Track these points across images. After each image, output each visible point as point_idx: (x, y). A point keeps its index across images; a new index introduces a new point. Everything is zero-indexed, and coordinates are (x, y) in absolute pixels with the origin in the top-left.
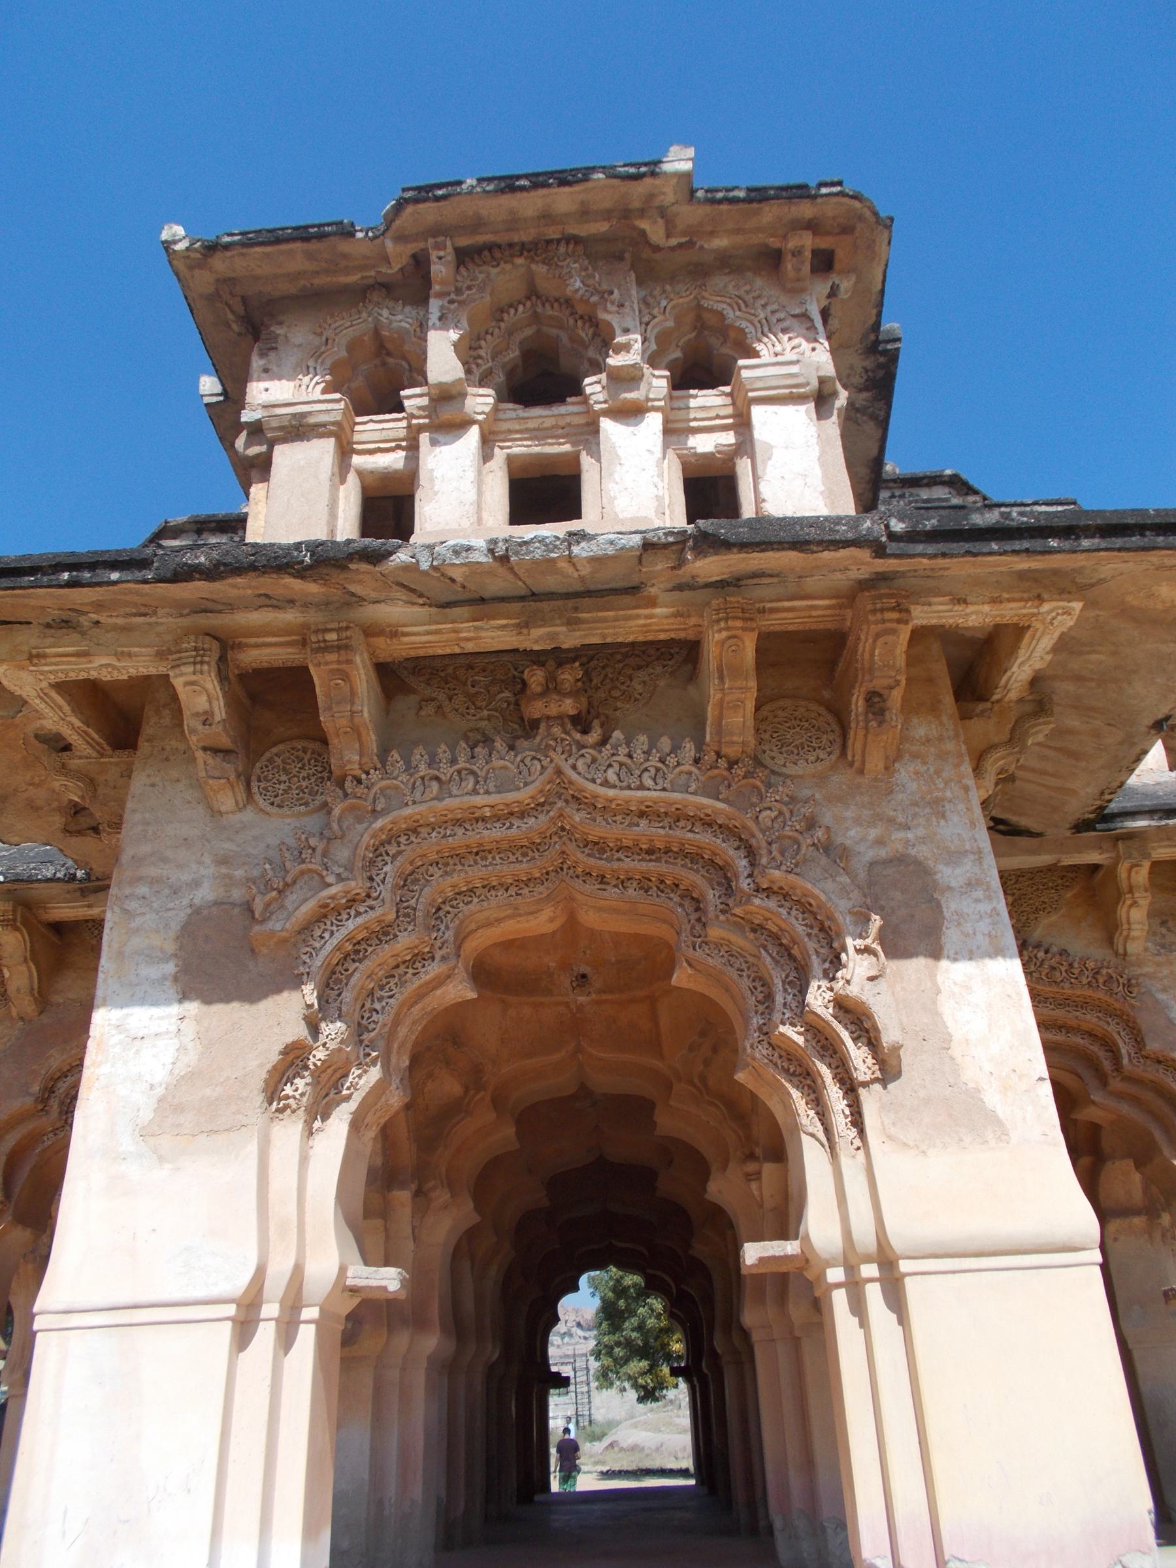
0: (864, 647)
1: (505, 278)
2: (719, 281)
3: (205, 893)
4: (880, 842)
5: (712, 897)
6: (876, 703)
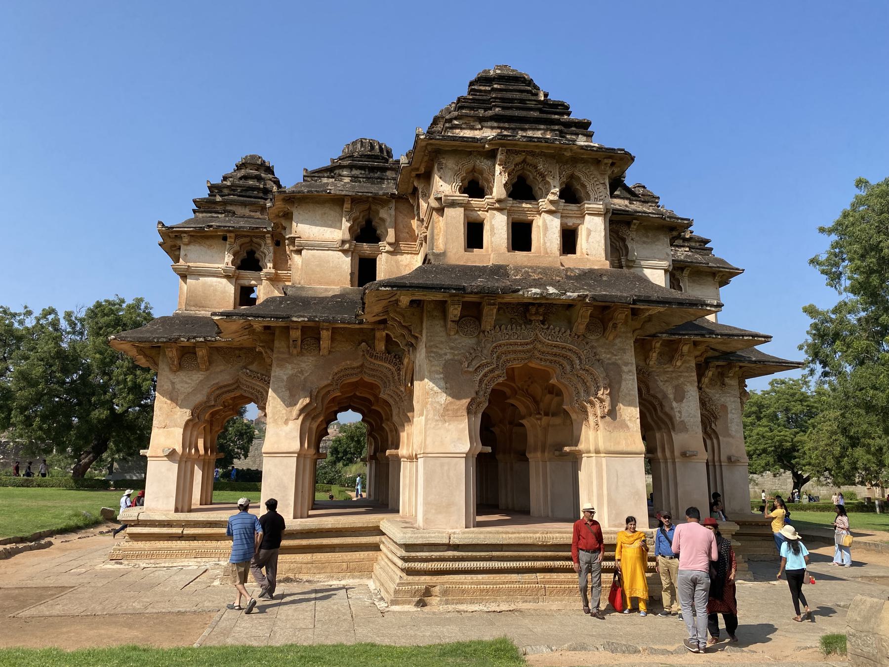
0: (616, 314)
1: (519, 159)
2: (580, 166)
3: (448, 357)
4: (609, 359)
5: (568, 368)
6: (615, 326)
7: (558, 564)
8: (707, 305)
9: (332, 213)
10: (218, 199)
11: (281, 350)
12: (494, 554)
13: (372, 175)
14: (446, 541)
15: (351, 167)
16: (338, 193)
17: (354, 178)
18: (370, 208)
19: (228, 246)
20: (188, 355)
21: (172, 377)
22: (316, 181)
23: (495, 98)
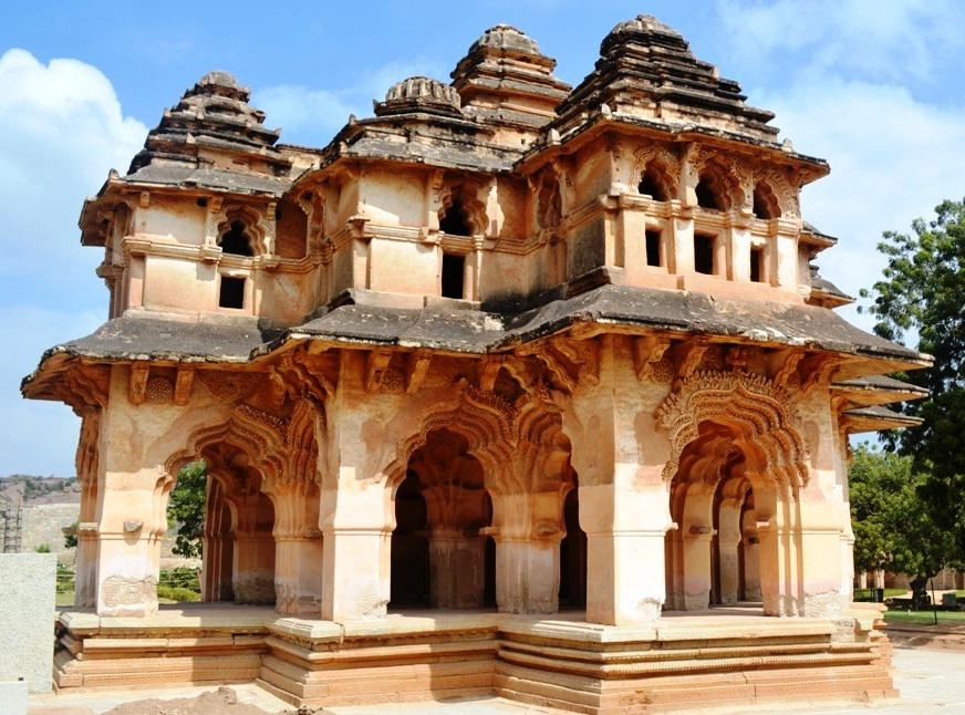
3: (640, 408)
4: (807, 416)
7: (766, 659)
8: (920, 359)
9: (411, 187)
10: (191, 140)
11: (354, 383)
12: (704, 651)
13: (457, 138)
14: (653, 638)
15: (430, 123)
16: (434, 163)
17: (438, 141)
18: (460, 187)
19: (210, 216)
20: (156, 380)
21: (132, 411)
22: (382, 138)
23: (664, 68)
